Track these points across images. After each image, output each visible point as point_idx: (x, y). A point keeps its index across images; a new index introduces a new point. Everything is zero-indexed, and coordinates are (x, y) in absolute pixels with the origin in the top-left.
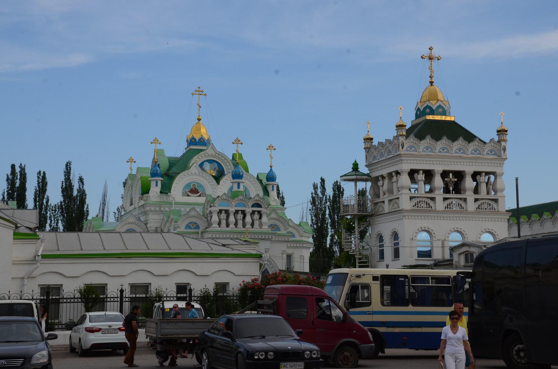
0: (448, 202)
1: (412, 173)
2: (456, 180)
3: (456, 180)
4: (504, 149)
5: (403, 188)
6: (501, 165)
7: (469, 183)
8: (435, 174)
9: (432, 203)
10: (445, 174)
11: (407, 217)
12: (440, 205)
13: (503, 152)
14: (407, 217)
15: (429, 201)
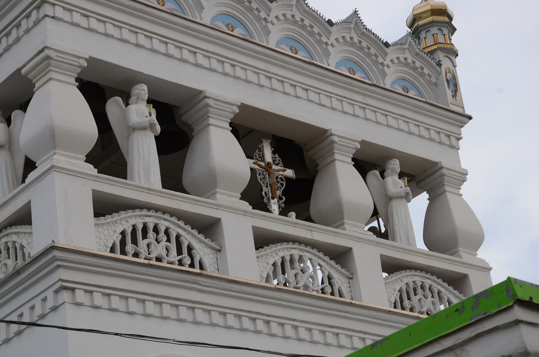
0: (276, 253)
1: (99, 89)
2: (290, 173)
3: (290, 173)
4: (454, 83)
5: (52, 139)
6: (453, 141)
7: (347, 184)
8: (205, 116)
9: (202, 251)
10: (248, 130)
11: (80, 296)
12: (242, 261)
13: (449, 93)
14: (80, 296)
15: (189, 237)
